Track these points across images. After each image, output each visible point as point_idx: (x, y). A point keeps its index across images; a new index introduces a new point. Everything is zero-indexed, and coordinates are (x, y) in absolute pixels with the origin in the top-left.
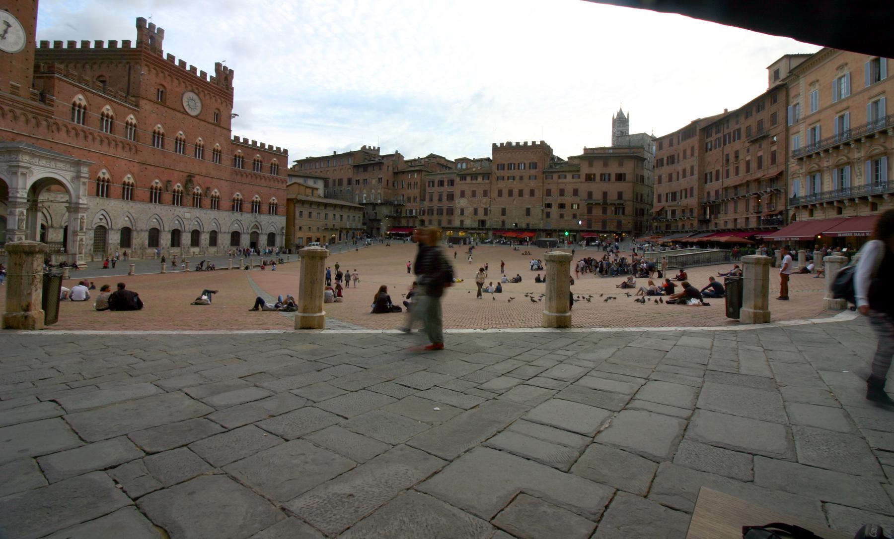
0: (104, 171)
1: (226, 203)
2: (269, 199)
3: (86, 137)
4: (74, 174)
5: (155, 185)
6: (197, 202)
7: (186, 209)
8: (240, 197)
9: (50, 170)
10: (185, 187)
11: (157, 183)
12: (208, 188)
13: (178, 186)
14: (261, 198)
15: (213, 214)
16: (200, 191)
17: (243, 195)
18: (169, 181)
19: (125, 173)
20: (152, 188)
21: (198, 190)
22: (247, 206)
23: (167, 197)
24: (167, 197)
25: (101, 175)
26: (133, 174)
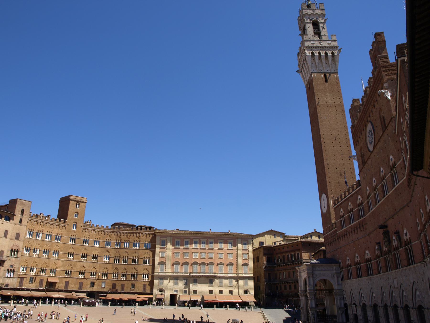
19: (365, 250)
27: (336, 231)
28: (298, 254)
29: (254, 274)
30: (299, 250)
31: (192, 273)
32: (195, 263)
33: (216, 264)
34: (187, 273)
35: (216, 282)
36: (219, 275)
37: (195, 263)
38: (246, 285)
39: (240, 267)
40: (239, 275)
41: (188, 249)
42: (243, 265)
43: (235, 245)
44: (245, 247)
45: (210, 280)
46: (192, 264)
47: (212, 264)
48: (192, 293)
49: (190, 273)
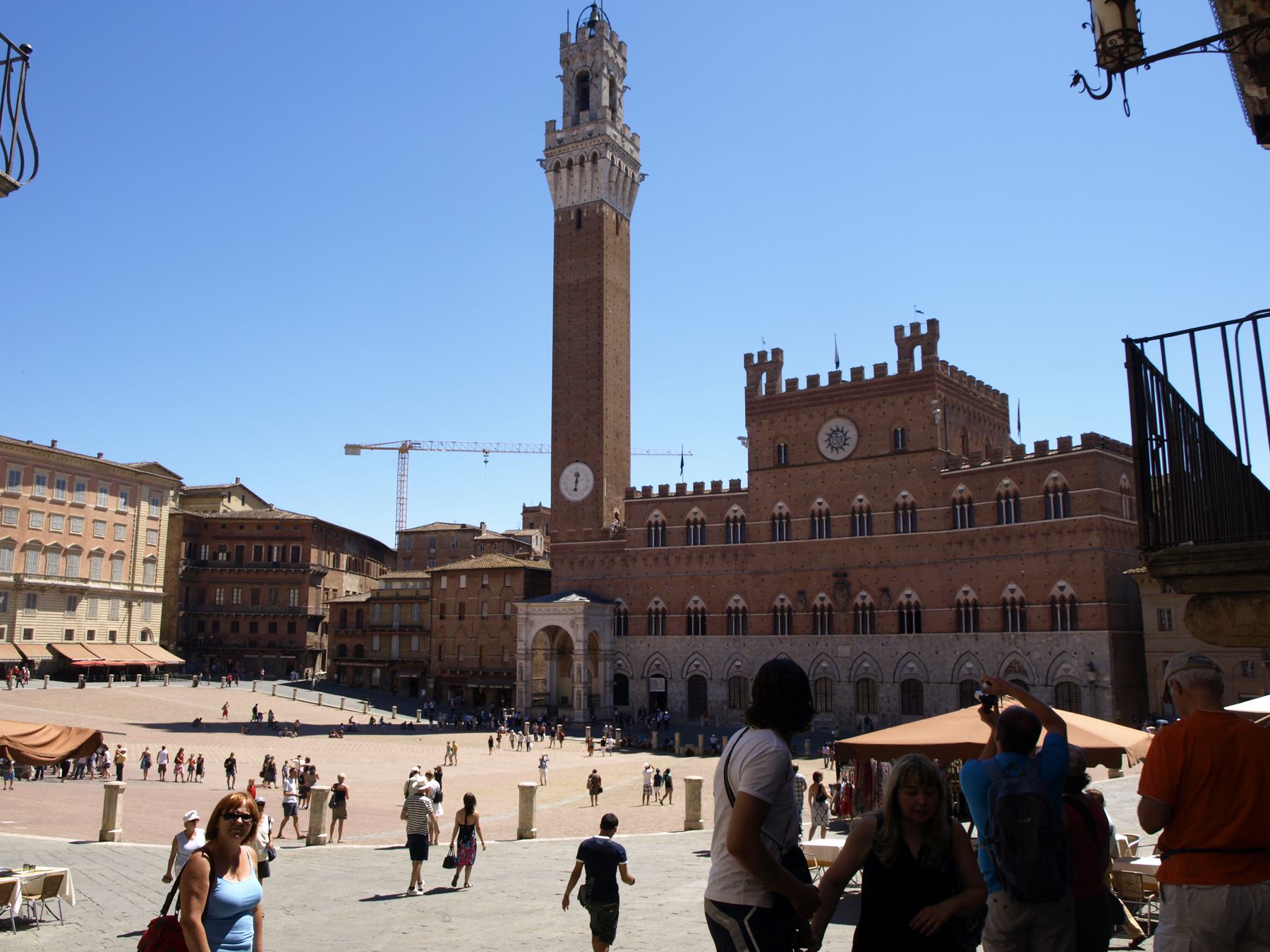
0: (696, 598)
1: (937, 613)
2: (1048, 587)
3: (667, 559)
4: (572, 617)
5: (778, 604)
6: (865, 621)
7: (838, 638)
8: (972, 596)
9: (547, 617)
10: (833, 597)
11: (783, 600)
12: (885, 591)
13: (821, 598)
14: (1025, 589)
15: (907, 643)
16: (867, 601)
17: (978, 591)
18: (802, 593)
19: (731, 594)
20: (775, 610)
21: (863, 597)
22: (989, 614)
23: (802, 618)
24: (802, 618)
25: (691, 605)
26: (743, 593)
27: (624, 545)
28: (296, 550)
29: (164, 588)
30: (302, 539)
31: (26, 575)
32: (35, 546)
33: (86, 552)
34: (8, 575)
35: (84, 605)
36: (91, 585)
37: (35, 546)
38: (146, 617)
39: (139, 564)
40: (137, 589)
41: (16, 496)
42: (146, 561)
43: (133, 502)
44: (155, 511)
45: (69, 598)
46: (25, 548)
47: (77, 550)
48: (19, 639)
49: (17, 576)
